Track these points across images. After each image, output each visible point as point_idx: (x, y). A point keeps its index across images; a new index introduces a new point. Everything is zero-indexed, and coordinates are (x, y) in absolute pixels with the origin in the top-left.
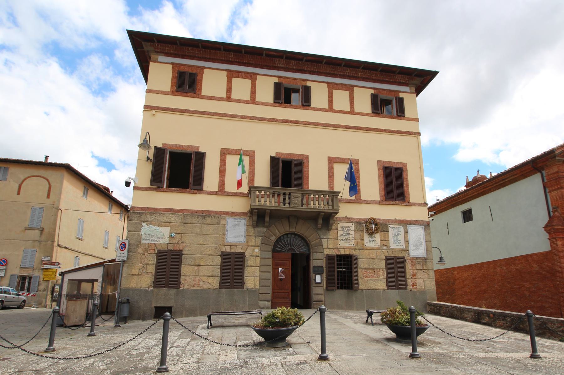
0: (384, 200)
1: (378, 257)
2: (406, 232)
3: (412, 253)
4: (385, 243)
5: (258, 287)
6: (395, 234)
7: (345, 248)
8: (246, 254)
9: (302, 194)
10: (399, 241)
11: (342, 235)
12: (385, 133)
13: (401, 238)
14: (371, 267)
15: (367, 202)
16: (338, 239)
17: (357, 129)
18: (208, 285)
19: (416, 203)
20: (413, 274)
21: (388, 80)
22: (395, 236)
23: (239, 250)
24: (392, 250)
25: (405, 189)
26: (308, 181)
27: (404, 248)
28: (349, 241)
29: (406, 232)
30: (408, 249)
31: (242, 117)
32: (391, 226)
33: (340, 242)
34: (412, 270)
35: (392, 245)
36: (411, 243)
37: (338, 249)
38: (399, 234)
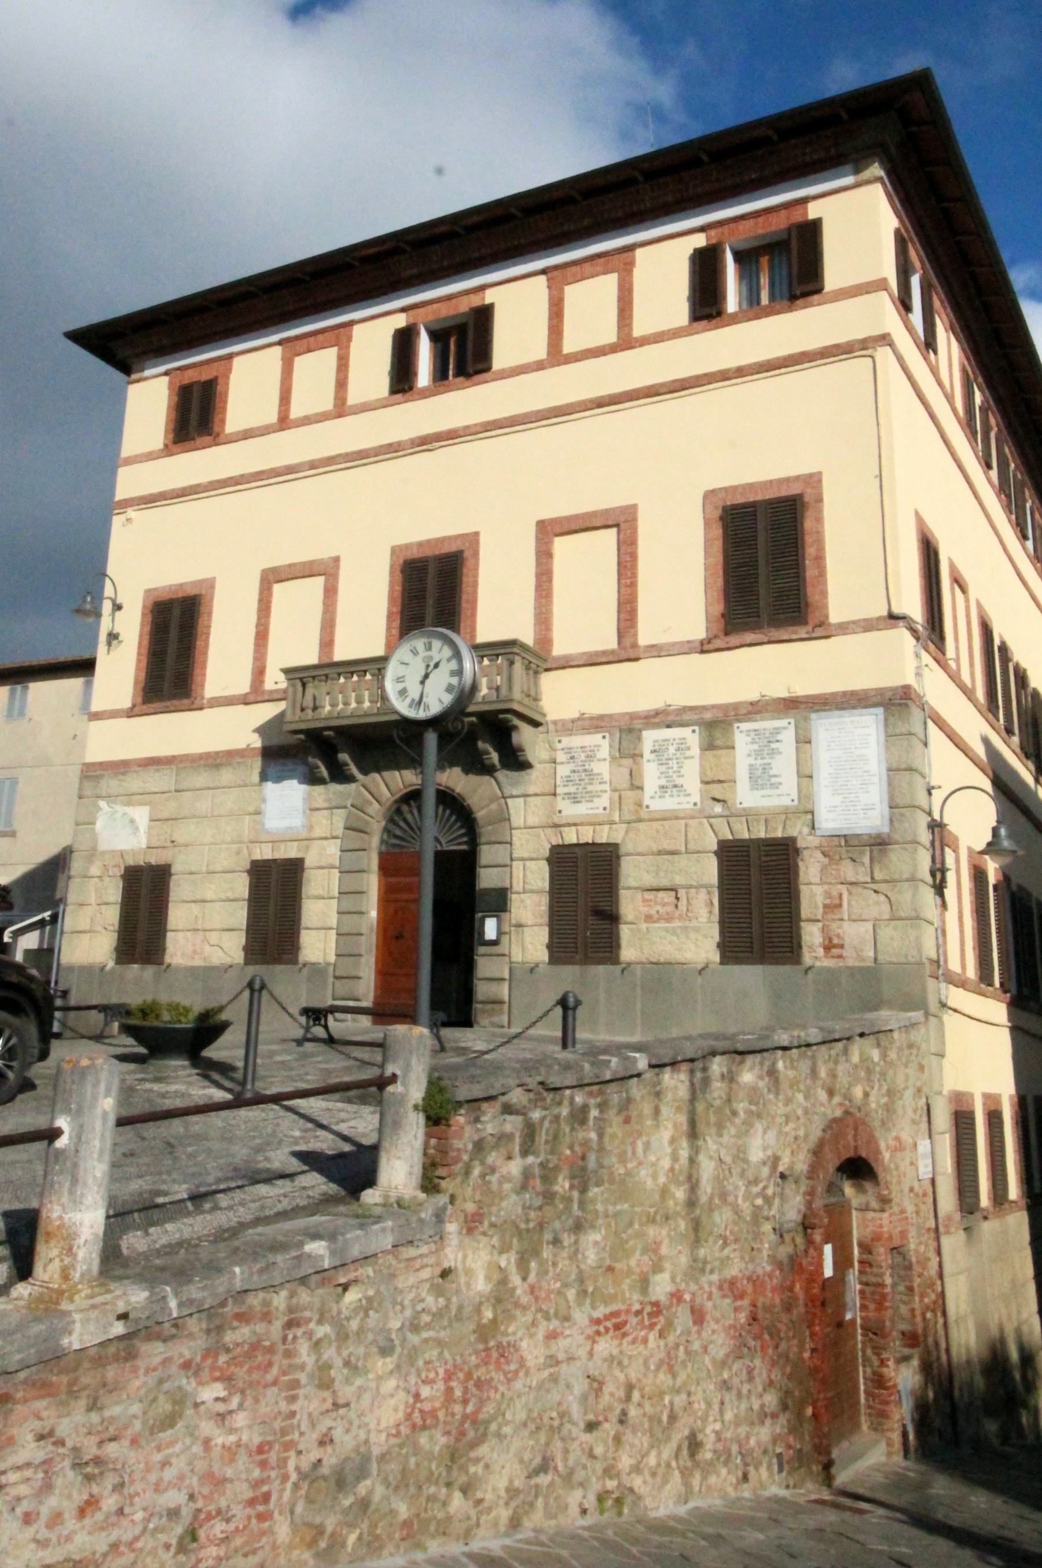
0: (721, 634)
1: (692, 846)
2: (804, 740)
3: (827, 820)
4: (717, 791)
5: (332, 959)
6: (759, 754)
7: (577, 821)
8: (308, 863)
9: (301, 679)
10: (773, 780)
11: (568, 780)
12: (739, 380)
13: (784, 765)
14: (665, 882)
15: (657, 651)
16: (555, 795)
17: (638, 399)
18: (220, 953)
19: (854, 622)
20: (828, 901)
21: (754, 176)
22: (759, 762)
23: (291, 852)
24: (749, 815)
25: (810, 573)
26: (474, 615)
27: (796, 803)
28: (592, 796)
29: (804, 740)
30: (809, 807)
31: (313, 465)
32: (745, 726)
33: (562, 804)
34: (826, 887)
35: (746, 797)
36: (876, 780)
37: (556, 826)
38: (773, 753)
